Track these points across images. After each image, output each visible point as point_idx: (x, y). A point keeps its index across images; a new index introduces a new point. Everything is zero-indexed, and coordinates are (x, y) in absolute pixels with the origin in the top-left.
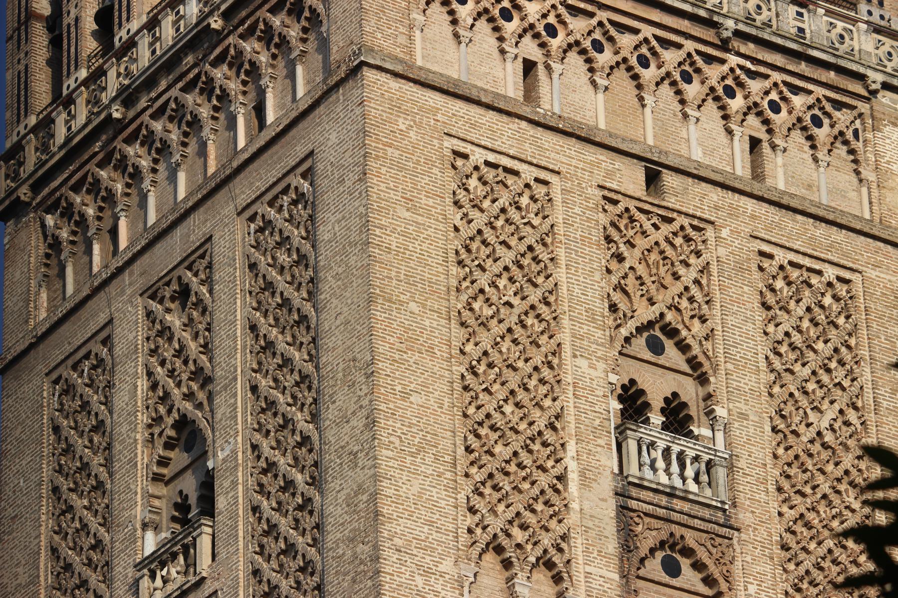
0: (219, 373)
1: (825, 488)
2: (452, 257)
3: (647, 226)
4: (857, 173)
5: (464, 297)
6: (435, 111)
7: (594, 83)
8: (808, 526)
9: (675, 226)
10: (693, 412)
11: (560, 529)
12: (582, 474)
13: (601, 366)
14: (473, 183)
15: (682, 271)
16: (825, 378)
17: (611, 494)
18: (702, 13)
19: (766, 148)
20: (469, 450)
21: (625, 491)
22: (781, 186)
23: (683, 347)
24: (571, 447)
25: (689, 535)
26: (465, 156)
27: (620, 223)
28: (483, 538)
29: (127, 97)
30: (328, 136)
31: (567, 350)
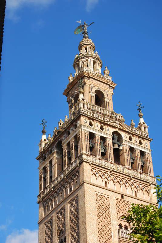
0: (66, 223)
2: (96, 208)
3: (122, 203)
4: (149, 195)
5: (98, 213)
6: (94, 188)
7: (114, 184)
9: (125, 203)
10: (128, 227)
12: (114, 236)
14: (99, 198)
15: (126, 208)
17: (118, 238)
18: (128, 175)
19: (137, 192)
20: (99, 233)
21: (120, 238)
22: (139, 197)
24: (112, 232)
26: (98, 194)
29: (54, 187)
30: (80, 192)
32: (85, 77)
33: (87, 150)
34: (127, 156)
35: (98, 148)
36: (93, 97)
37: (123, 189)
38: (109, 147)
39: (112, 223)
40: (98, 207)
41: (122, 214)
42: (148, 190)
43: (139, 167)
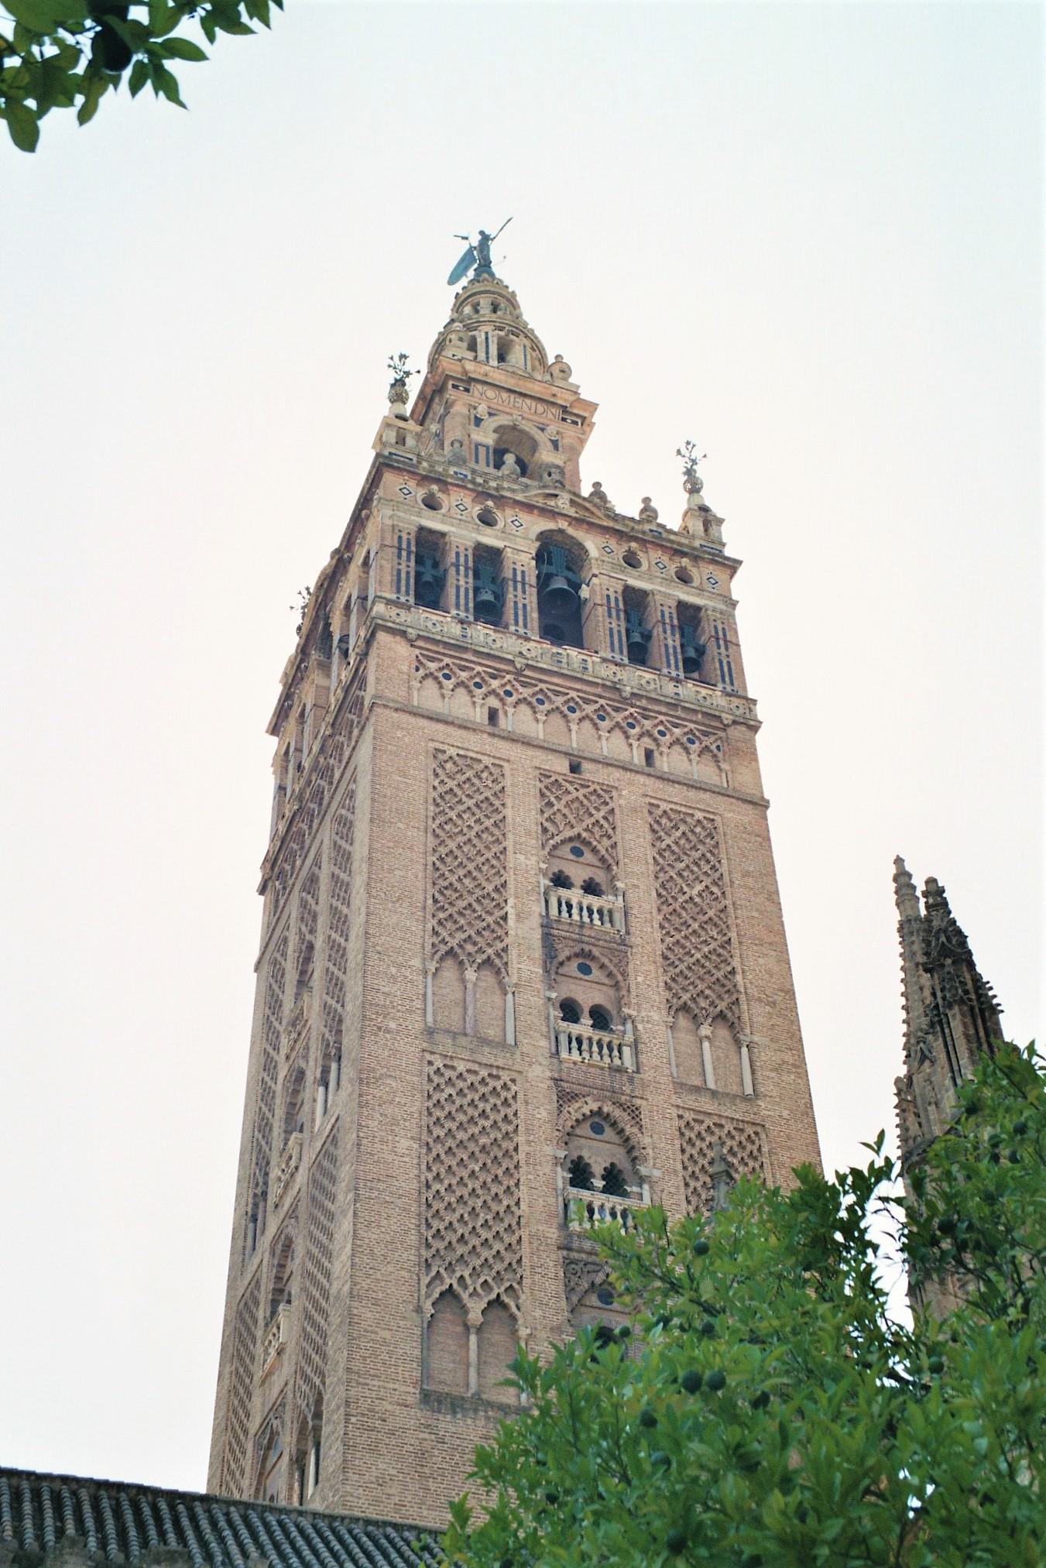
1: (695, 926)
2: (431, 801)
3: (571, 788)
5: (438, 822)
9: (591, 789)
10: (604, 888)
11: (500, 945)
12: (518, 915)
13: (534, 858)
16: (695, 869)
19: (656, 754)
20: (435, 901)
21: (547, 926)
23: (594, 850)
24: (511, 902)
27: (550, 787)
28: (443, 949)
31: (510, 849)
32: (451, 383)
33: (403, 589)
34: (610, 616)
35: (462, 583)
36: (482, 451)
37: (579, 737)
38: (515, 582)
39: (510, 865)
40: (439, 800)
42: (718, 747)
43: (672, 658)
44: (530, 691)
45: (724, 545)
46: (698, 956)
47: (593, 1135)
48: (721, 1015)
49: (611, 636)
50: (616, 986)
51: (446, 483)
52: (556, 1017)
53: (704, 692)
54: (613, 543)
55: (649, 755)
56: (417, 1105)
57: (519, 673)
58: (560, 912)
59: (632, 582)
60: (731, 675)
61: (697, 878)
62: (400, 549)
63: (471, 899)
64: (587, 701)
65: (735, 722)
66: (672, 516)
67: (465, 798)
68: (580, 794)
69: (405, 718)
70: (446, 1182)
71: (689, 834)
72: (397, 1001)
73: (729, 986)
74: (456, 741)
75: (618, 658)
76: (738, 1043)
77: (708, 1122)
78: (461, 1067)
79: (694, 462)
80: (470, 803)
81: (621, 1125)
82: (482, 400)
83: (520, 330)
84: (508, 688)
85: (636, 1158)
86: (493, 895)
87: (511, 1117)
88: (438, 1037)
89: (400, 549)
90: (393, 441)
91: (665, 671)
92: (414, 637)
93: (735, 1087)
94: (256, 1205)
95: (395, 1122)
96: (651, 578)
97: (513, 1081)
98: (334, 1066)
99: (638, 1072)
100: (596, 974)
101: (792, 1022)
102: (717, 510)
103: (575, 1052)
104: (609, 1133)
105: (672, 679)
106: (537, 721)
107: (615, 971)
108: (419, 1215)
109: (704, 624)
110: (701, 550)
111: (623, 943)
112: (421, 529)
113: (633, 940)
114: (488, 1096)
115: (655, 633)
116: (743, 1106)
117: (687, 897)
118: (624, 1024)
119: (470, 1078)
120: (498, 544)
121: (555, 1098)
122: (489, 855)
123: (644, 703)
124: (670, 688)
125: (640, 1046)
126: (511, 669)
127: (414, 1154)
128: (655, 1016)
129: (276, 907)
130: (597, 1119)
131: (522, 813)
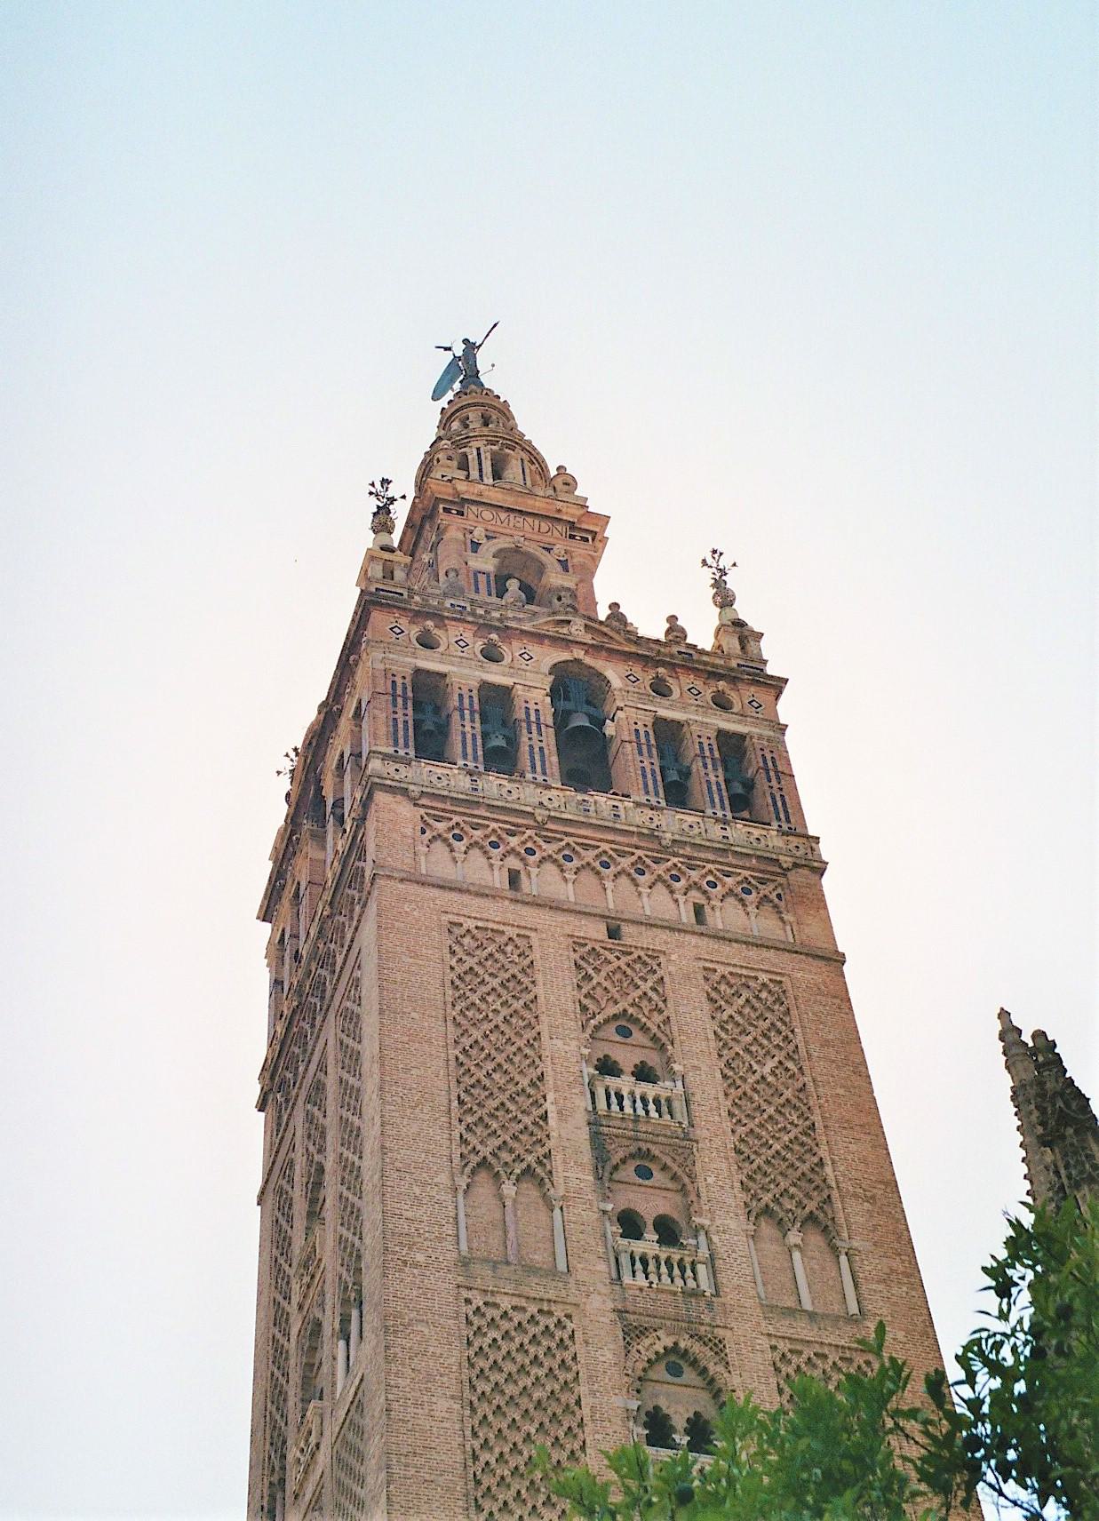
1: (771, 1110)
3: (611, 957)
4: (782, 919)
5: (458, 1008)
8: (759, 1137)
11: (541, 1151)
12: (560, 1113)
13: (574, 1043)
16: (765, 1042)
19: (707, 909)
20: (461, 1102)
21: (594, 1123)
24: (550, 1097)
25: (652, 1147)
27: (585, 959)
28: (475, 1159)
33: (401, 741)
34: (641, 753)
35: (468, 729)
37: (616, 896)
38: (529, 723)
39: (544, 1054)
40: (458, 982)
41: (612, 1010)
42: (779, 896)
44: (555, 846)
45: (765, 662)
46: (777, 1146)
47: (669, 1378)
48: (811, 1218)
49: (644, 776)
50: (683, 1190)
51: (442, 618)
52: (614, 1234)
53: (756, 833)
54: (637, 670)
55: (698, 911)
56: (455, 1355)
57: (540, 827)
58: (609, 1105)
59: (663, 713)
60: (786, 812)
61: (768, 1052)
62: (394, 696)
63: (503, 1098)
64: (622, 854)
65: (796, 865)
66: (702, 633)
67: (489, 980)
68: (622, 963)
69: (413, 889)
70: (497, 1450)
71: (754, 1001)
72: (424, 1227)
73: (818, 1181)
74: (474, 911)
75: (653, 800)
76: (835, 1250)
77: (808, 1352)
78: (506, 1303)
79: (723, 572)
80: (495, 983)
81: (703, 1363)
82: (479, 523)
83: (517, 442)
84: (529, 845)
85: (724, 1403)
86: (529, 1090)
87: (569, 1362)
88: (476, 1268)
89: (394, 696)
90: (380, 575)
91: (709, 812)
92: (416, 794)
93: (836, 1307)
94: (273, 1498)
95: (430, 1378)
96: (684, 708)
97: (569, 1316)
98: (355, 1313)
99: (717, 1295)
100: (659, 1177)
101: (898, 1221)
102: (754, 624)
103: (640, 1275)
104: (689, 1375)
105: (717, 820)
106: (566, 880)
107: (680, 1172)
108: (466, 1495)
109: (750, 754)
110: (740, 670)
111: (687, 1137)
112: (418, 671)
113: (699, 1133)
114: (539, 1337)
115: (694, 768)
116: (848, 1329)
117: (757, 1076)
118: (696, 1237)
119: (517, 1317)
120: (507, 681)
121: (621, 1335)
122: (521, 1043)
123: (688, 851)
124: (716, 832)
125: (719, 1263)
126: (532, 823)
127: (455, 1417)
128: (733, 1225)
129: (279, 1125)
130: (673, 1358)
131: (556, 990)
